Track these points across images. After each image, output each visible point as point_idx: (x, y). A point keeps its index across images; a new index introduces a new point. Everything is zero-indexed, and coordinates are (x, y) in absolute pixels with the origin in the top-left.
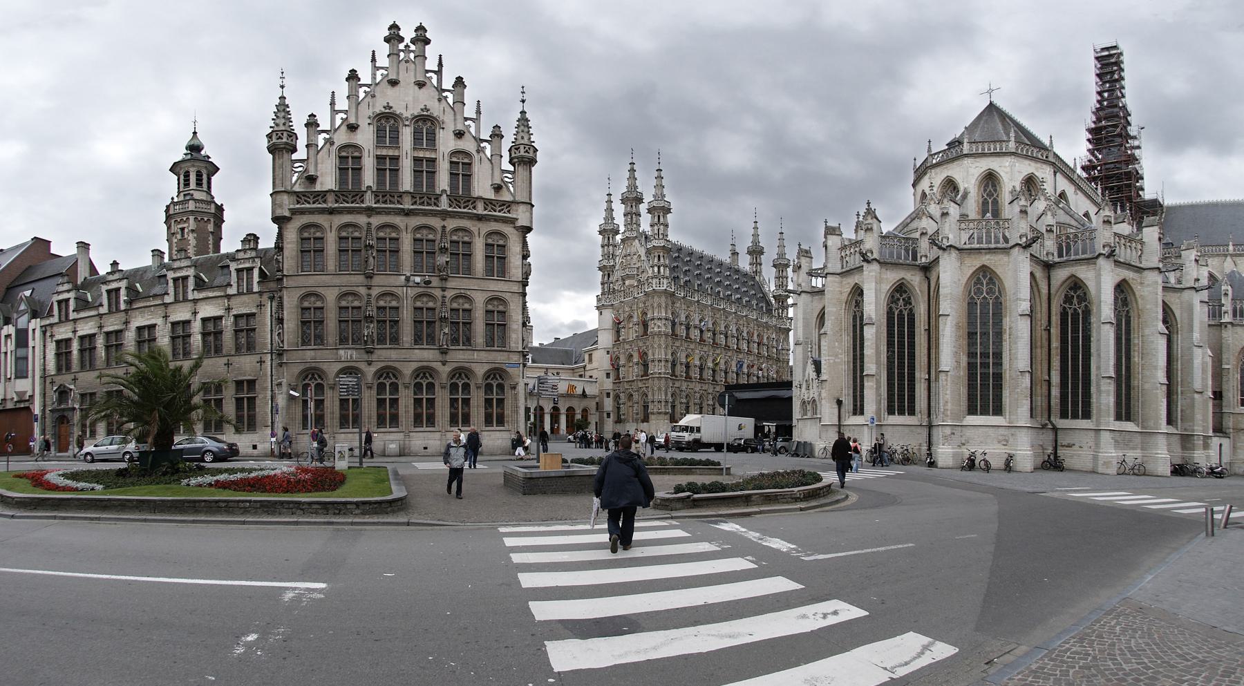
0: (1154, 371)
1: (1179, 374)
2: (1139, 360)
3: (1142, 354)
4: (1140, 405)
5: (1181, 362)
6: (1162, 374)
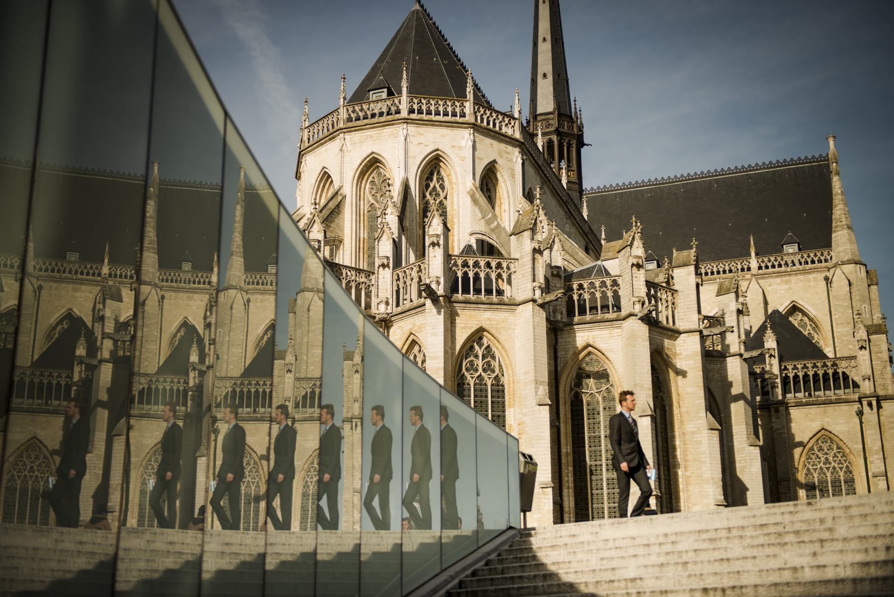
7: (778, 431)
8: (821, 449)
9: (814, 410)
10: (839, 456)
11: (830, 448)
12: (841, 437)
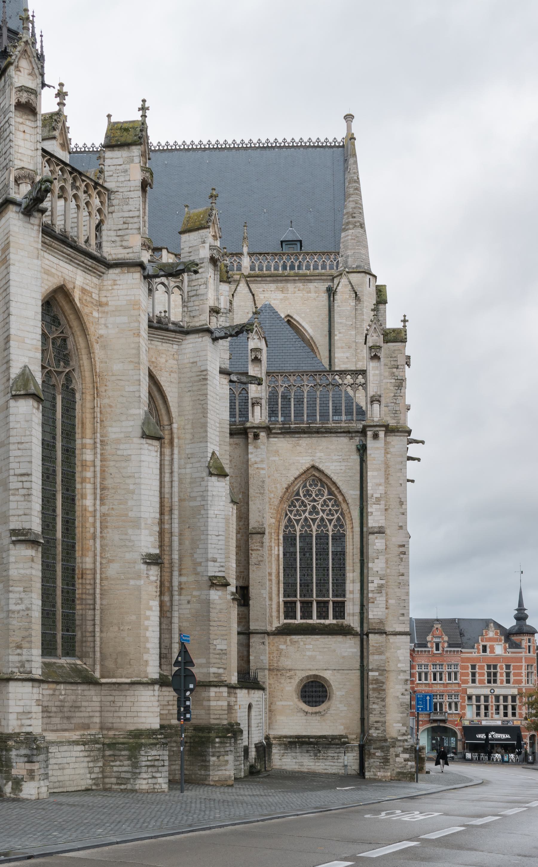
0: (130, 531)
1: (176, 544)
2: (95, 505)
3: (102, 489)
4: (98, 618)
5: (180, 514)
6: (152, 539)
7: (256, 466)
8: (308, 494)
9: (305, 442)
10: (330, 504)
11: (320, 493)
12: (335, 478)
